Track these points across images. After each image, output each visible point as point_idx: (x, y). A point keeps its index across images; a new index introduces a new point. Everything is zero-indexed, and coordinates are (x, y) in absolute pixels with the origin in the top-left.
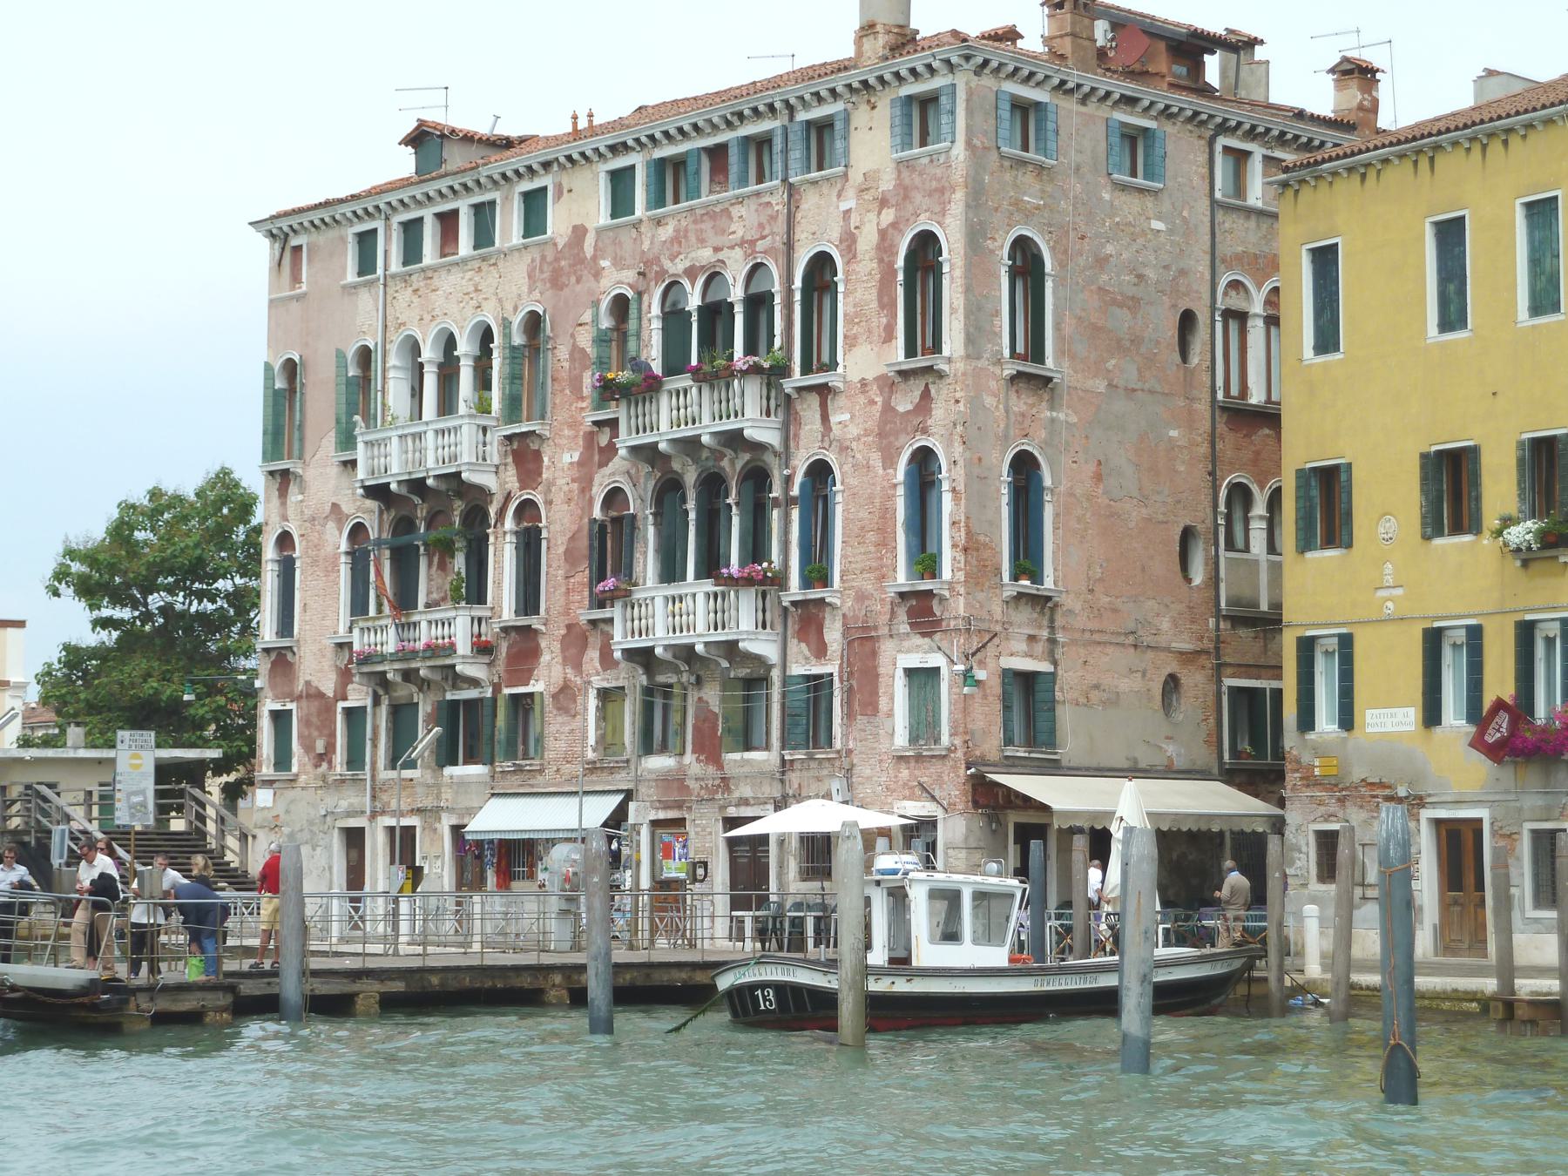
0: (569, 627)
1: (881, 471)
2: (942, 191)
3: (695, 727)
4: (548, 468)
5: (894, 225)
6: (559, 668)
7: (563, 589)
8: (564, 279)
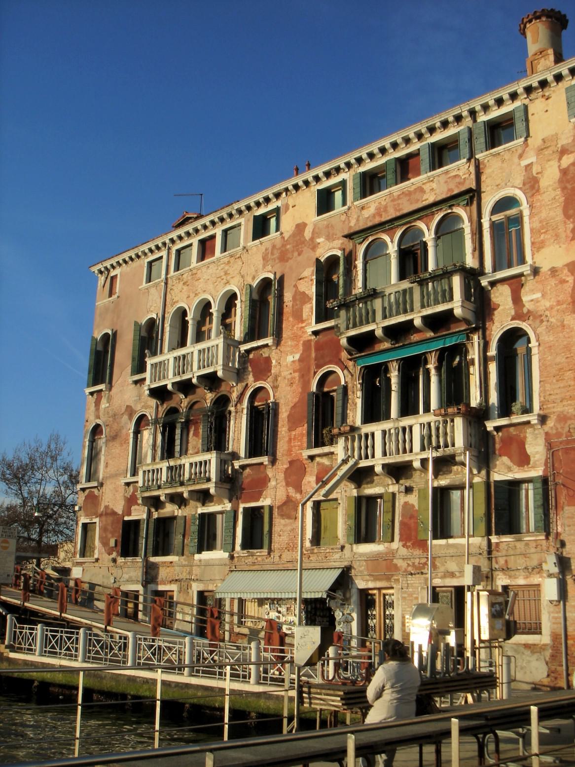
0: (291, 463)
3: (402, 523)
4: (276, 366)
7: (287, 439)
8: (289, 255)
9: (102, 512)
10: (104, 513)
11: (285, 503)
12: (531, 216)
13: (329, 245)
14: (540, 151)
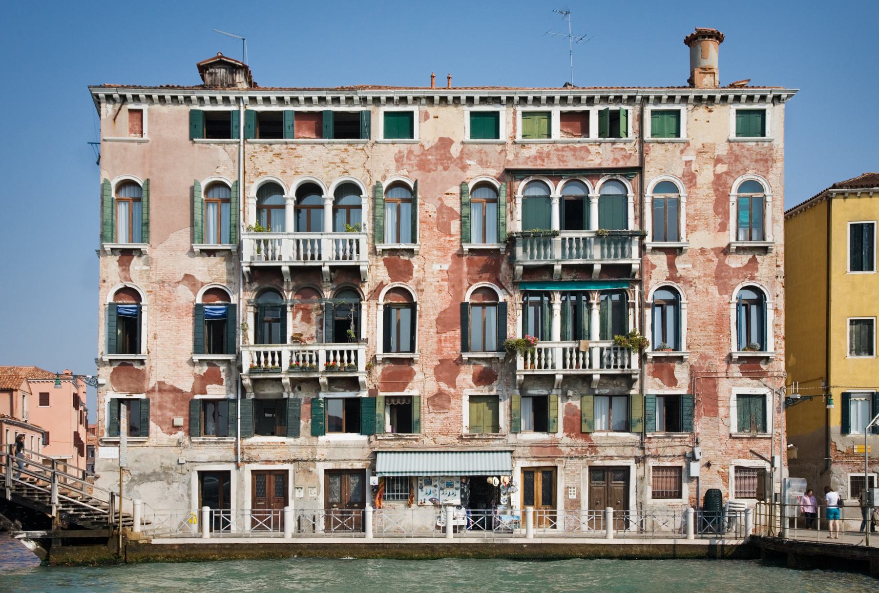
1: (718, 296)
2: (766, 161)
3: (565, 419)
5: (727, 173)
6: (435, 383)
7: (436, 339)
9: (154, 388)
10: (157, 389)
11: (436, 395)
12: (688, 203)
13: (481, 170)
14: (700, 153)
